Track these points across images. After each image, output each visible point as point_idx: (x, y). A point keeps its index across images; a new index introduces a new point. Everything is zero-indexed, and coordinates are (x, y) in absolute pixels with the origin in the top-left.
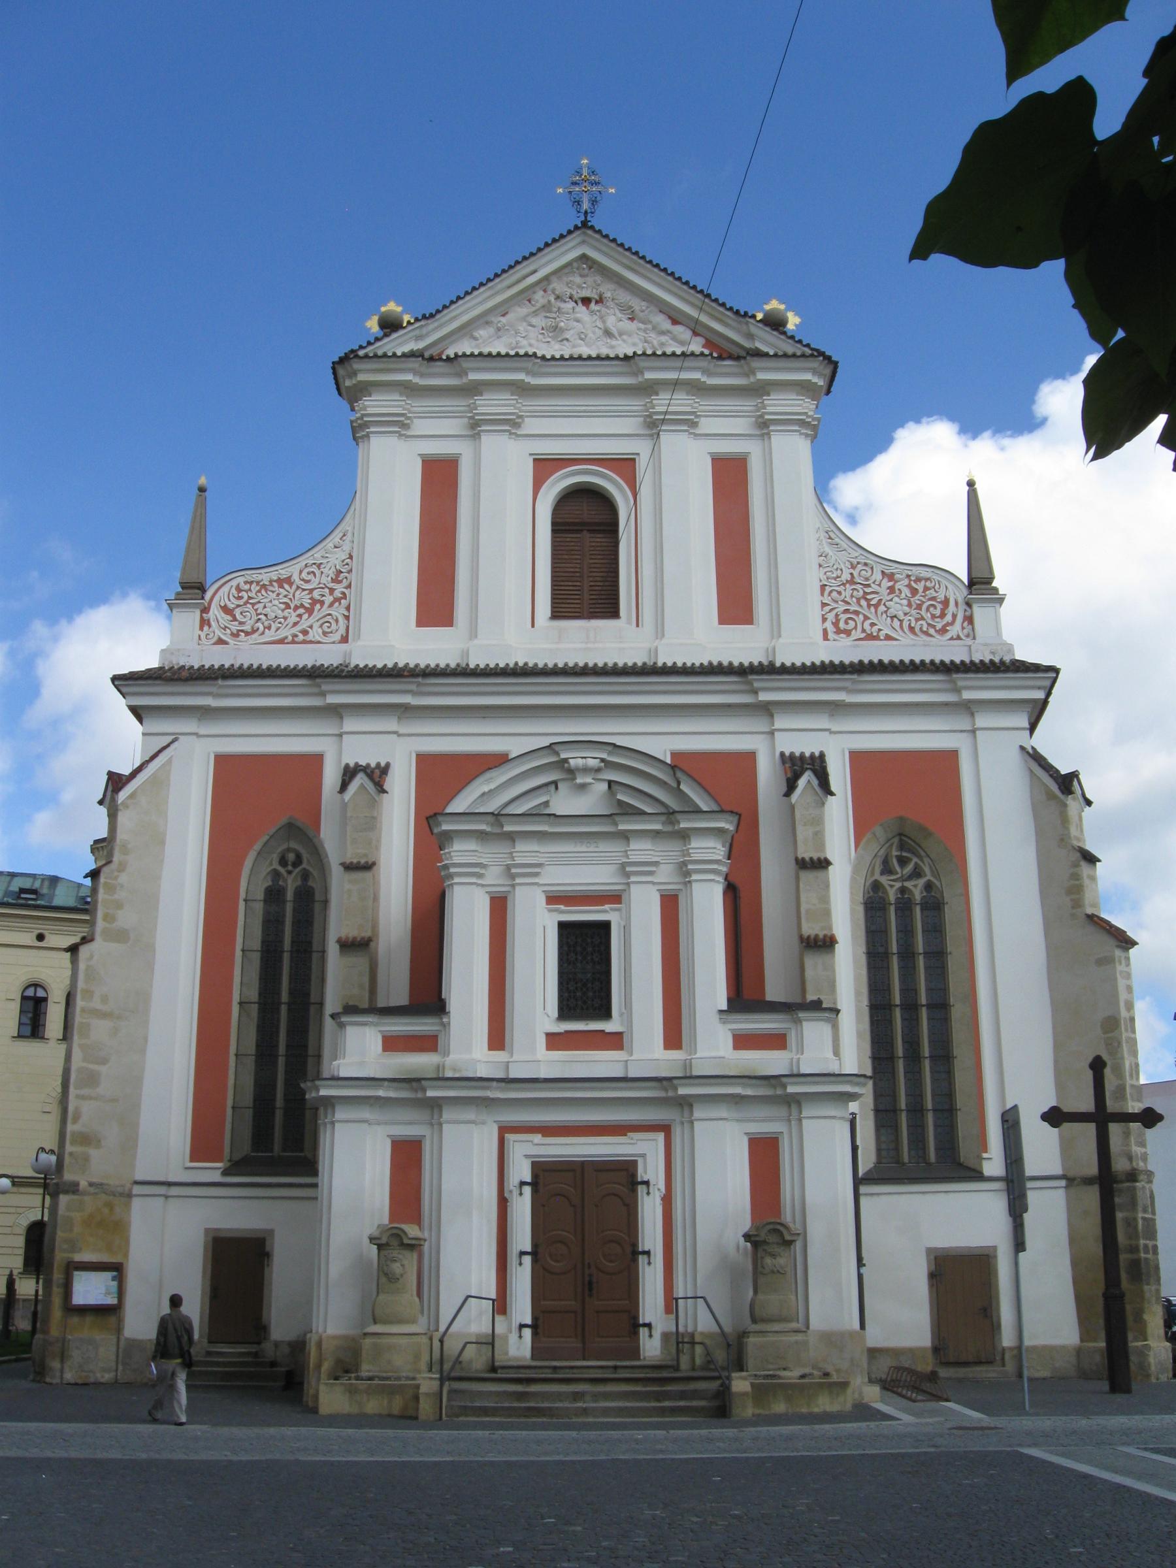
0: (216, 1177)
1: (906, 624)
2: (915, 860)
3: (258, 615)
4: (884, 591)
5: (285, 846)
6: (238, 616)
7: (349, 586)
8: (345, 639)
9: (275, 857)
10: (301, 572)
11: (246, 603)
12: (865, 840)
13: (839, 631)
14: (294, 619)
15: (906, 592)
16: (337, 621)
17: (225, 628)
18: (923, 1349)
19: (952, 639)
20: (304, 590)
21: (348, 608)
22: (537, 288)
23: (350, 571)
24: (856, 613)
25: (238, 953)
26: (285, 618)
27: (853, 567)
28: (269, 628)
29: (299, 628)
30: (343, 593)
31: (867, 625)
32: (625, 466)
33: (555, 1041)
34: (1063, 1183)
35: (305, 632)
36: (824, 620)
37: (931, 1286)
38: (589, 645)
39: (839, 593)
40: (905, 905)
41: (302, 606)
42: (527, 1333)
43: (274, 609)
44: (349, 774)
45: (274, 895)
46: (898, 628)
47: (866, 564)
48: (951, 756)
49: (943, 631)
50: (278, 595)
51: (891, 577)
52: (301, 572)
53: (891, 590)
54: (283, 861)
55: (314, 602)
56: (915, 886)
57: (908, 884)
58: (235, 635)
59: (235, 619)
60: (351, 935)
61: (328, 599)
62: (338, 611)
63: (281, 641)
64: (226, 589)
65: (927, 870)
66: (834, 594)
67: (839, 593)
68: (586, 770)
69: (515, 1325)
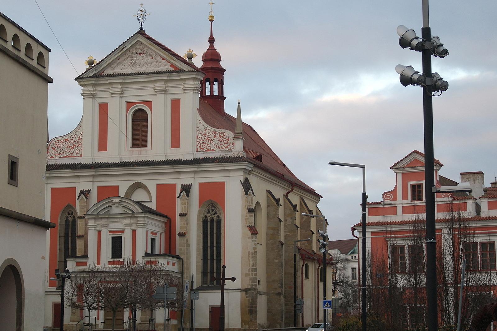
0: (55, 290)
1: (218, 146)
2: (215, 210)
3: (61, 149)
4: (213, 137)
5: (68, 210)
6: (56, 150)
7: (82, 141)
8: (81, 156)
9: (67, 213)
10: (70, 137)
11: (58, 146)
12: (201, 207)
13: (201, 149)
14: (68, 151)
15: (218, 136)
16: (79, 150)
17: (53, 153)
18: (207, 328)
19: (229, 150)
20: (72, 142)
21: (82, 147)
22: (127, 51)
23: (82, 137)
24: (205, 143)
25: (58, 238)
26: (67, 150)
27: (205, 130)
28: (63, 153)
29: (70, 153)
30: (81, 143)
31: (208, 147)
32: (149, 104)
33: (110, 263)
34: (240, 291)
35: (72, 154)
36: (197, 146)
37: (210, 314)
38: (139, 156)
39: (201, 138)
40: (212, 222)
41: (71, 146)
42: (103, 324)
43: (64, 148)
44: (82, 192)
45: (67, 222)
46: (216, 147)
47: (209, 129)
48: (223, 184)
49: (227, 147)
50: (65, 144)
51: (215, 133)
52: (70, 137)
53: (215, 136)
54: (69, 214)
55: (74, 145)
56: (215, 216)
57: (213, 216)
58: (55, 155)
59: (55, 151)
60: (80, 234)
61: (77, 145)
62: (79, 148)
63: (66, 157)
64: (53, 142)
65: (218, 212)
66: (200, 138)
67: (201, 138)
68: (116, 203)
69: (100, 322)
